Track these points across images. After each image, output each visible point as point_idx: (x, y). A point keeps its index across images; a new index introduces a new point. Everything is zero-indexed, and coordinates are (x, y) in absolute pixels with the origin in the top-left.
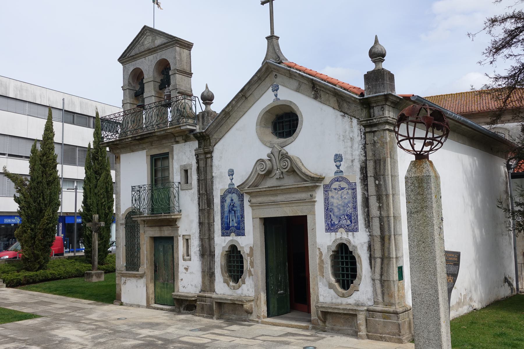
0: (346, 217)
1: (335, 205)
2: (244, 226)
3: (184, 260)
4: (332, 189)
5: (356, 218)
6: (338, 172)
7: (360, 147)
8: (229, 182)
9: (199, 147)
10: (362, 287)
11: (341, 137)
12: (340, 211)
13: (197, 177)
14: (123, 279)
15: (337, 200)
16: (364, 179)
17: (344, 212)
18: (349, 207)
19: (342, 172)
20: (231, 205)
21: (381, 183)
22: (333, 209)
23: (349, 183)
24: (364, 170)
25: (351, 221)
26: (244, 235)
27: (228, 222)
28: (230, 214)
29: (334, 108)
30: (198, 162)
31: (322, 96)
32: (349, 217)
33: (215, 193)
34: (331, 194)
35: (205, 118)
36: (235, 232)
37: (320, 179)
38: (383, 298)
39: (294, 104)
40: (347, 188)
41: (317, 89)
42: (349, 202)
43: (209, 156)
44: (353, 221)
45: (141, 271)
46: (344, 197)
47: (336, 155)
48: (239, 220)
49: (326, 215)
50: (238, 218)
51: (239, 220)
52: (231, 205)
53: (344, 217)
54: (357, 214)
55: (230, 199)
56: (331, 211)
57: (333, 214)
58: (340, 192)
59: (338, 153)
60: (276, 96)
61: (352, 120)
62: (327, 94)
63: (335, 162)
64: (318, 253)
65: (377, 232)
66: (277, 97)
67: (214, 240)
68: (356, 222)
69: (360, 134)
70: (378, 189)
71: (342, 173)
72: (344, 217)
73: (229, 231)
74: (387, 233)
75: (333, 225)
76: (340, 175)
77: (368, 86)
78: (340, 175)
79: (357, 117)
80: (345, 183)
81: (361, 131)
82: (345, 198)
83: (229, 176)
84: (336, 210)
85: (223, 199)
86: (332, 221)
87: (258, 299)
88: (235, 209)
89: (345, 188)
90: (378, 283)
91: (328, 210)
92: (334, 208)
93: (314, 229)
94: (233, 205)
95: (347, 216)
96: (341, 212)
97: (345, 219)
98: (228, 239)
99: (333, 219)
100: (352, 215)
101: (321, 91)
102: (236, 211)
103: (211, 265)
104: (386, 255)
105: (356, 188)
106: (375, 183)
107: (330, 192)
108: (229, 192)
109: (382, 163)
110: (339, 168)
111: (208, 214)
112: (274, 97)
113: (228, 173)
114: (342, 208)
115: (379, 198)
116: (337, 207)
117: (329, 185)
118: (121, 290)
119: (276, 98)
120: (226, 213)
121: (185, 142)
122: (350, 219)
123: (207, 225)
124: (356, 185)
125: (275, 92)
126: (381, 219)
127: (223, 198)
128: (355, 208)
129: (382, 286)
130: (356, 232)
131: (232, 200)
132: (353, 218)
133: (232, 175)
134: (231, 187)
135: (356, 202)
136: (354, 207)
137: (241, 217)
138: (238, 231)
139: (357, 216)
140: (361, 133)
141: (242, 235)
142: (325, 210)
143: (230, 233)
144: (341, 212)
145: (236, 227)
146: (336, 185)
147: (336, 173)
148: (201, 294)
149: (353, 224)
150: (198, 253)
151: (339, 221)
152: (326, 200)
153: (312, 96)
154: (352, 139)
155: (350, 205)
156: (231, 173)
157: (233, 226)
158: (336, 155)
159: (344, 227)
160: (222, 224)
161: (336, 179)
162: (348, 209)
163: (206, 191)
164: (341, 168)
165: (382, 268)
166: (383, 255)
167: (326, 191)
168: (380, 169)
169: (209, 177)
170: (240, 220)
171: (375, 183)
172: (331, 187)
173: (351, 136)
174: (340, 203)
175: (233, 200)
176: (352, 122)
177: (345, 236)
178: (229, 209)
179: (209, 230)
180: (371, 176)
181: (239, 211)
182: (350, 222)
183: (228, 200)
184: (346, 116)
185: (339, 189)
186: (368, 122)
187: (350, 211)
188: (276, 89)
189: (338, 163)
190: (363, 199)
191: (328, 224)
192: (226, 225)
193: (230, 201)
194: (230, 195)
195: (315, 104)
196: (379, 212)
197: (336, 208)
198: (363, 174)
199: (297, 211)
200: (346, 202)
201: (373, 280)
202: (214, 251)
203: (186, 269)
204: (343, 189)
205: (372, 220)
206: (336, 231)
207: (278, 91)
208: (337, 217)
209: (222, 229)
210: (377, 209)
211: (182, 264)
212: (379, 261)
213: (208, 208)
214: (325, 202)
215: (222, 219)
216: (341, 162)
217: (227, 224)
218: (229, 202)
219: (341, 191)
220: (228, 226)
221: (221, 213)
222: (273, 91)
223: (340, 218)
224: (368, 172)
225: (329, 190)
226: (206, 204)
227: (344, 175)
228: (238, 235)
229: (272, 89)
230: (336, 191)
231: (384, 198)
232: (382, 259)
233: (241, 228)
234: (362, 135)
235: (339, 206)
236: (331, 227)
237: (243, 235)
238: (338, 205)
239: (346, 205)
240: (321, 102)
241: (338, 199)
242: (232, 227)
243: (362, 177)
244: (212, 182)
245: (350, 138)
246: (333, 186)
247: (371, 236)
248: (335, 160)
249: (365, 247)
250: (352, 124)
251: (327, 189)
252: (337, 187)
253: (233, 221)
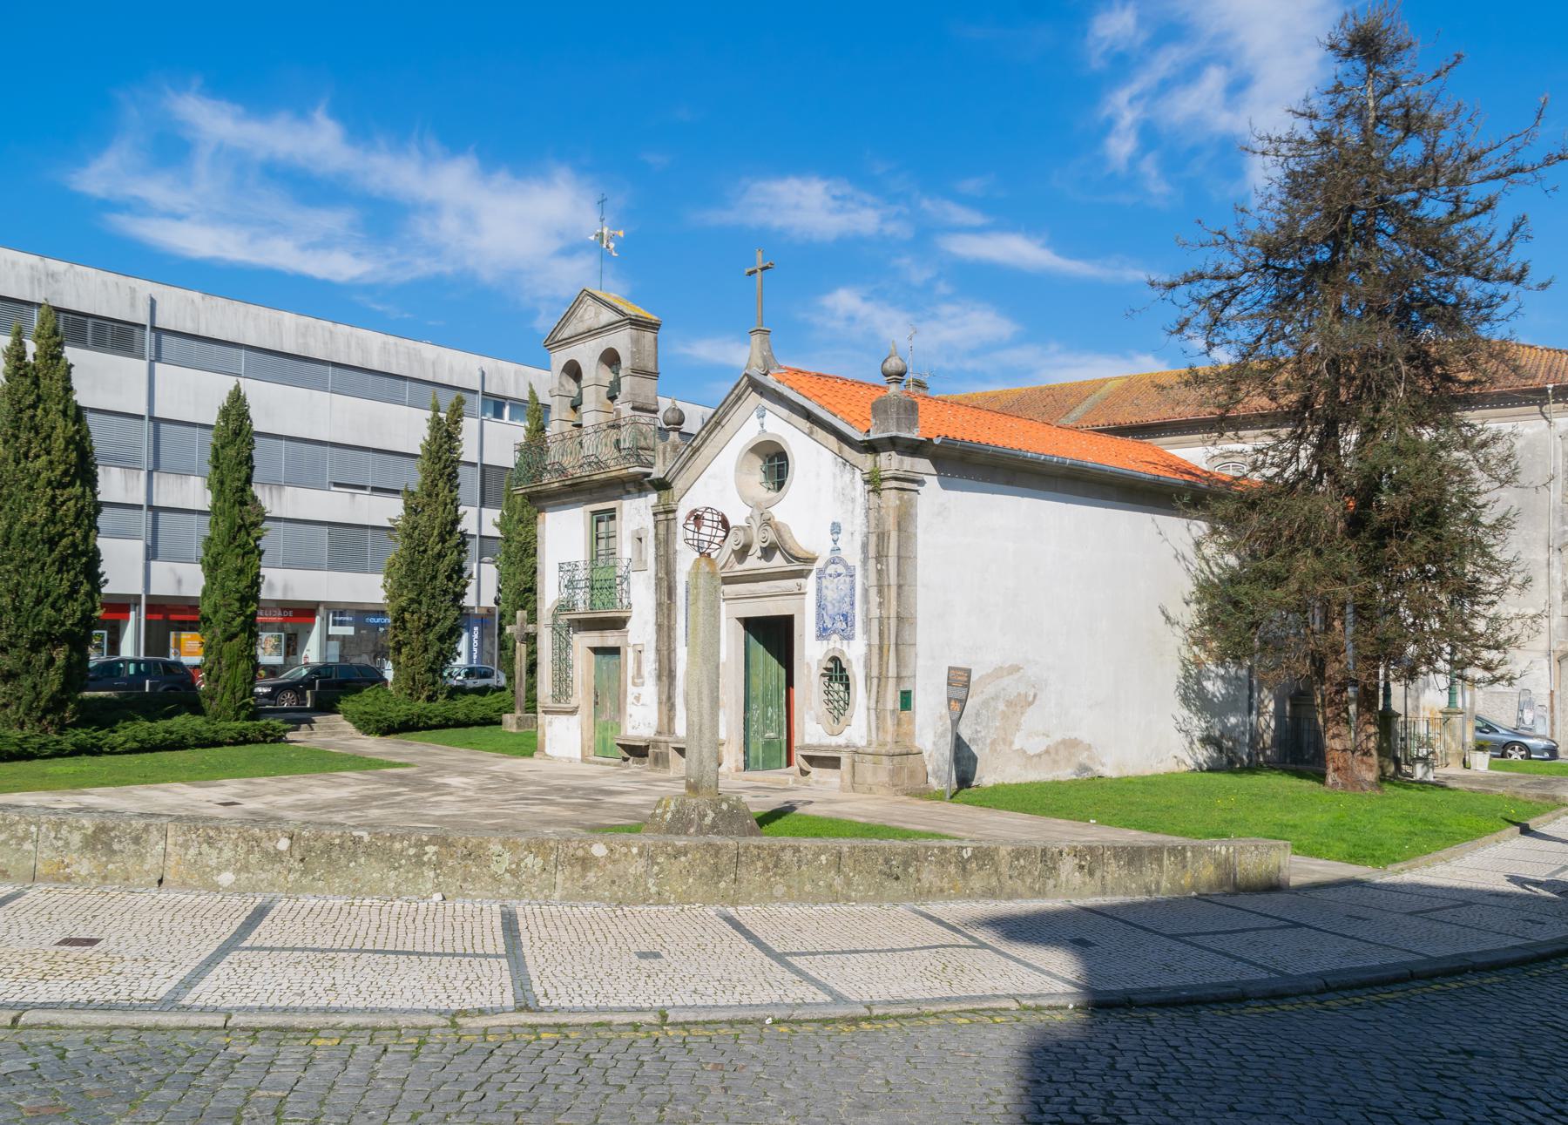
1: (829, 599)
3: (634, 684)
9: (659, 501)
10: (854, 722)
14: (549, 717)
23: (847, 567)
24: (865, 546)
30: (656, 527)
33: (678, 578)
37: (812, 560)
43: (671, 516)
45: (574, 702)
47: (834, 523)
60: (762, 425)
65: (875, 640)
68: (853, 625)
74: (886, 642)
75: (825, 629)
76: (836, 554)
78: (836, 554)
84: (830, 607)
90: (872, 712)
118: (544, 735)
126: (881, 619)
129: (878, 718)
146: (831, 569)
150: (654, 673)
152: (819, 590)
155: (848, 599)
158: (834, 523)
164: (839, 544)
166: (880, 673)
169: (671, 552)
177: (838, 645)
179: (669, 637)
201: (868, 709)
203: (638, 698)
204: (839, 575)
211: (631, 690)
212: (875, 681)
227: (843, 554)
232: (879, 679)
236: (823, 633)
239: (842, 600)
244: (675, 559)
246: (828, 571)
247: (869, 645)
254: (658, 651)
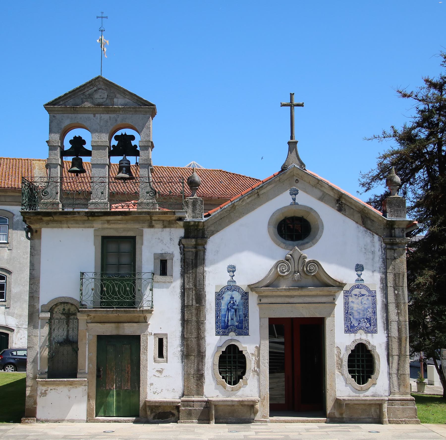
0: (366, 321)
1: (355, 309)
2: (248, 325)
7: (381, 261)
8: (229, 278)
11: (363, 249)
12: (360, 315)
13: (181, 269)
16: (385, 289)
17: (363, 316)
18: (369, 312)
19: (363, 280)
20: (230, 302)
21: (400, 293)
22: (352, 313)
23: (369, 291)
25: (370, 324)
26: (248, 335)
27: (226, 320)
28: (228, 312)
29: (357, 223)
31: (346, 210)
32: (369, 320)
34: (351, 299)
35: (198, 206)
38: (399, 389)
39: (315, 211)
41: (342, 203)
42: (369, 307)
44: (372, 324)
46: (364, 303)
47: (357, 265)
49: (346, 318)
50: (240, 317)
52: (230, 302)
53: (364, 320)
55: (230, 297)
56: (350, 315)
59: (360, 264)
60: (294, 200)
61: (374, 236)
62: (352, 210)
63: (356, 271)
64: (336, 352)
66: (295, 201)
67: (205, 340)
68: (375, 325)
69: (381, 249)
70: (397, 297)
71: (363, 281)
72: (364, 320)
76: (361, 283)
77: (391, 210)
78: (361, 283)
79: (379, 234)
80: (365, 291)
81: (382, 247)
84: (356, 314)
85: (219, 296)
86: (352, 323)
87: (264, 399)
89: (365, 295)
91: (348, 313)
93: (332, 330)
94: (233, 303)
97: (364, 322)
98: (225, 338)
100: (372, 319)
101: (346, 206)
103: (200, 367)
104: (403, 353)
105: (376, 296)
106: (395, 293)
107: (350, 298)
108: (228, 289)
109: (401, 276)
110: (360, 277)
111: (198, 312)
112: (292, 201)
114: (361, 312)
115: (398, 306)
116: (357, 311)
119: (294, 202)
120: (223, 311)
121: (164, 228)
122: (369, 322)
123: (194, 324)
124: (376, 293)
125: (294, 196)
127: (219, 295)
128: (374, 313)
130: (375, 333)
131: (232, 298)
132: (372, 321)
133: (233, 272)
134: (232, 284)
135: (376, 307)
139: (376, 320)
140: (382, 249)
141: (245, 335)
144: (361, 315)
145: (236, 326)
146: (356, 291)
147: (357, 280)
148: (184, 398)
149: (372, 327)
151: (359, 324)
152: (346, 303)
153: (337, 208)
154: (373, 253)
155: (370, 310)
157: (233, 325)
158: (357, 265)
160: (216, 322)
161: (357, 287)
162: (368, 313)
163: (195, 286)
164: (362, 277)
165: (399, 364)
167: (347, 296)
168: (399, 282)
170: (242, 319)
171: (395, 293)
172: (352, 293)
173: (373, 250)
174: (360, 307)
175: (233, 298)
176: (374, 238)
178: (228, 307)
180: (390, 286)
182: (370, 324)
183: (227, 297)
184: (369, 231)
186: (392, 241)
187: (370, 315)
188: (294, 193)
190: (382, 305)
191: (348, 326)
192: (223, 324)
193: (229, 299)
194: (229, 293)
195: (339, 215)
196: (397, 317)
197: (356, 312)
198: (383, 284)
199: (315, 313)
200: (366, 308)
202: (205, 352)
204: (363, 295)
205: (391, 323)
206: (355, 332)
208: (357, 320)
209: (217, 328)
210: (395, 315)
212: (396, 358)
213: (197, 305)
214: (345, 306)
215: (217, 317)
218: (227, 300)
221: (216, 311)
222: (291, 195)
224: (388, 283)
225: (349, 296)
226: (194, 300)
227: (365, 283)
228: (239, 334)
229: (290, 193)
231: (402, 306)
232: (399, 356)
233: (244, 327)
234: (383, 250)
235: (359, 311)
237: (247, 334)
238: (358, 309)
239: (366, 310)
240: (345, 215)
241: (358, 304)
242: (231, 326)
243: (382, 286)
245: (371, 252)
248: (356, 269)
249: (384, 346)
250: (373, 239)
251: (347, 295)
252: (358, 293)
253: (232, 319)
254: (183, 337)
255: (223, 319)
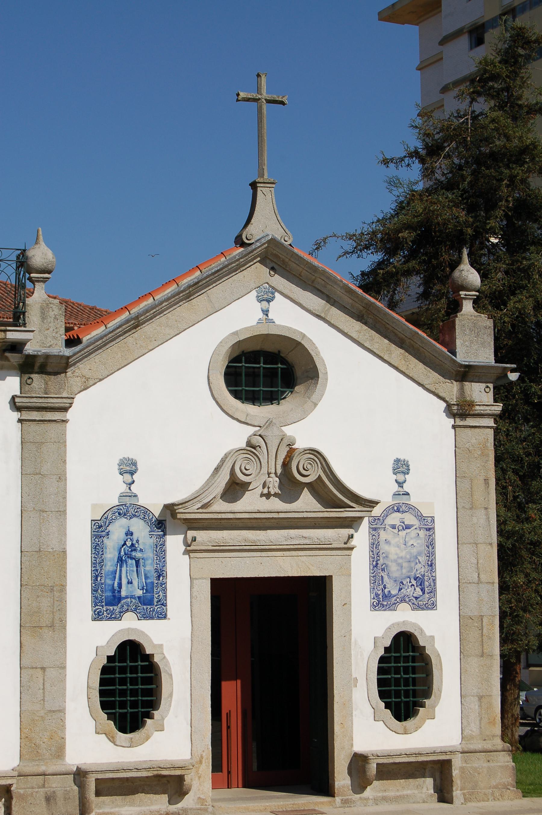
0: (414, 582)
1: (392, 557)
2: (166, 596)
4: (387, 526)
5: (432, 584)
6: (399, 495)
8: (123, 488)
15: (397, 549)
17: (409, 572)
19: (408, 494)
20: (125, 544)
23: (420, 517)
25: (423, 590)
26: (165, 617)
27: (116, 585)
28: (121, 567)
32: (420, 581)
36: (136, 609)
40: (417, 526)
42: (419, 554)
44: (426, 589)
47: (397, 461)
48: (149, 581)
49: (373, 577)
50: (146, 578)
51: (149, 581)
53: (410, 582)
54: (435, 577)
55: (124, 531)
56: (383, 570)
57: (388, 575)
58: (403, 533)
60: (266, 312)
63: (395, 474)
66: (267, 315)
72: (410, 582)
73: (117, 609)
76: (404, 499)
78: (404, 499)
82: (412, 545)
83: (121, 474)
84: (393, 568)
86: (385, 588)
88: (138, 555)
89: (412, 526)
92: (390, 564)
94: (133, 545)
95: (415, 580)
96: (404, 571)
97: (411, 586)
99: (387, 586)
100: (426, 578)
102: (141, 561)
107: (382, 532)
108: (119, 514)
110: (402, 487)
112: (261, 315)
113: (117, 467)
114: (405, 565)
116: (395, 561)
117: (381, 518)
119: (265, 317)
122: (421, 585)
125: (265, 303)
128: (431, 566)
131: (129, 533)
132: (427, 584)
133: (132, 473)
134: (128, 501)
136: (429, 563)
137: (155, 575)
138: (145, 607)
141: (159, 618)
142: (372, 567)
143: (120, 612)
144: (404, 571)
146: (394, 519)
151: (400, 590)
152: (374, 546)
155: (423, 559)
156: (128, 468)
158: (397, 461)
159: (410, 600)
160: (94, 590)
161: (396, 508)
162: (419, 566)
167: (375, 529)
170: (152, 583)
172: (386, 522)
174: (403, 554)
175: (132, 534)
181: (149, 562)
182: (422, 590)
185: (401, 528)
187: (423, 570)
189: (401, 478)
191: (377, 595)
193: (123, 536)
194: (123, 521)
197: (394, 564)
199: (310, 566)
200: (415, 554)
204: (408, 527)
206: (392, 607)
207: (270, 303)
208: (395, 581)
214: (372, 552)
215: (95, 578)
216: (406, 476)
217: (113, 590)
219: (405, 532)
220: (114, 596)
221: (94, 564)
222: (260, 301)
223: (402, 583)
227: (413, 500)
229: (258, 297)
230: (396, 531)
233: (156, 600)
235: (400, 561)
238: (398, 558)
241: (398, 547)
242: (127, 597)
252: (397, 523)
253: (130, 582)
255: (109, 582)
